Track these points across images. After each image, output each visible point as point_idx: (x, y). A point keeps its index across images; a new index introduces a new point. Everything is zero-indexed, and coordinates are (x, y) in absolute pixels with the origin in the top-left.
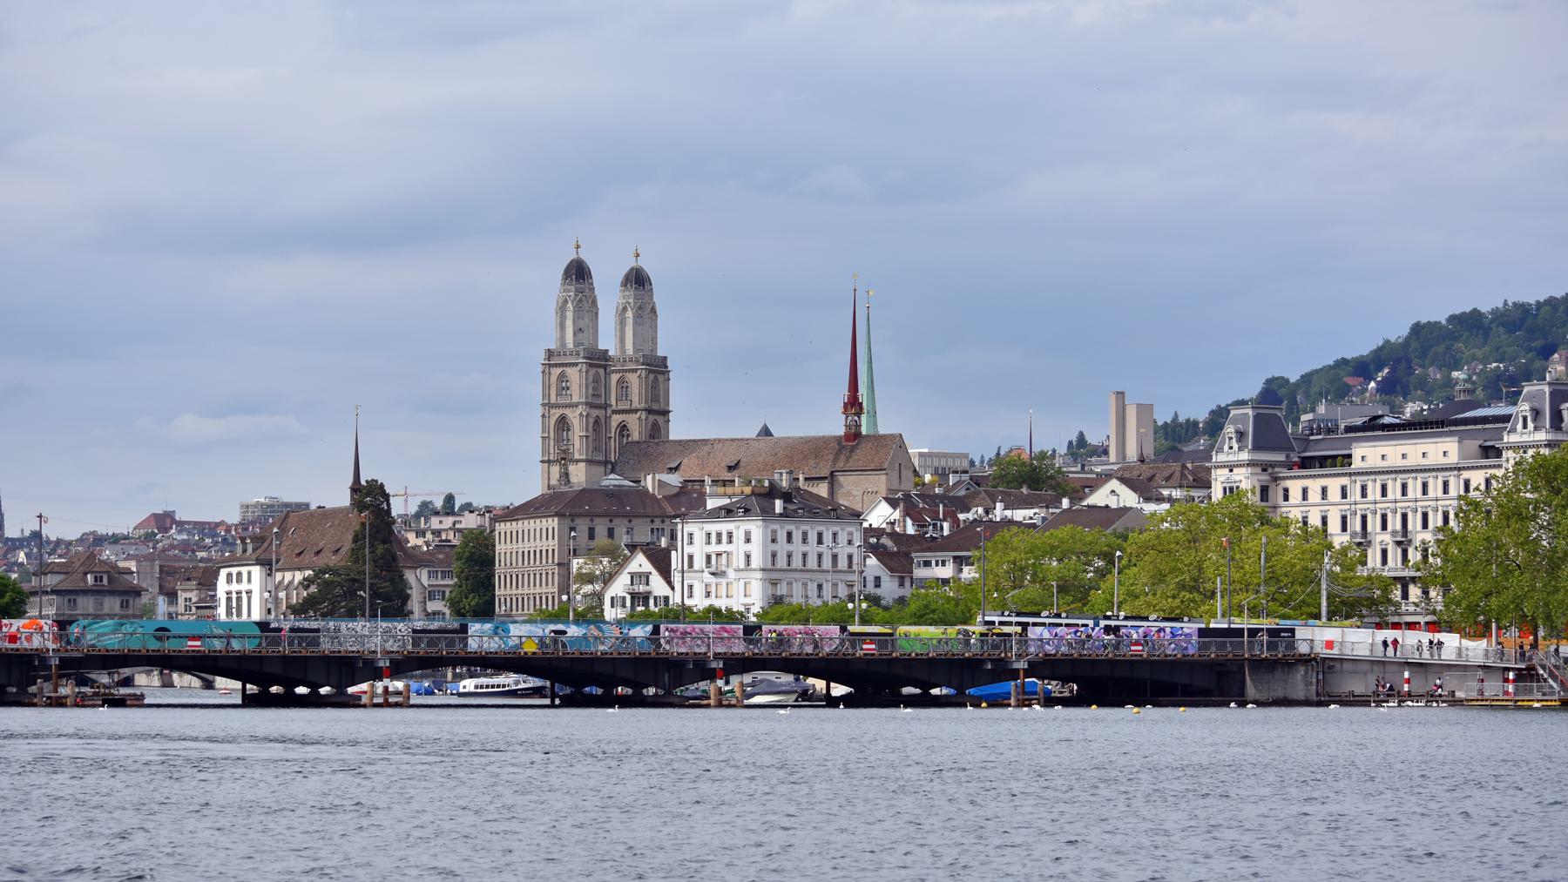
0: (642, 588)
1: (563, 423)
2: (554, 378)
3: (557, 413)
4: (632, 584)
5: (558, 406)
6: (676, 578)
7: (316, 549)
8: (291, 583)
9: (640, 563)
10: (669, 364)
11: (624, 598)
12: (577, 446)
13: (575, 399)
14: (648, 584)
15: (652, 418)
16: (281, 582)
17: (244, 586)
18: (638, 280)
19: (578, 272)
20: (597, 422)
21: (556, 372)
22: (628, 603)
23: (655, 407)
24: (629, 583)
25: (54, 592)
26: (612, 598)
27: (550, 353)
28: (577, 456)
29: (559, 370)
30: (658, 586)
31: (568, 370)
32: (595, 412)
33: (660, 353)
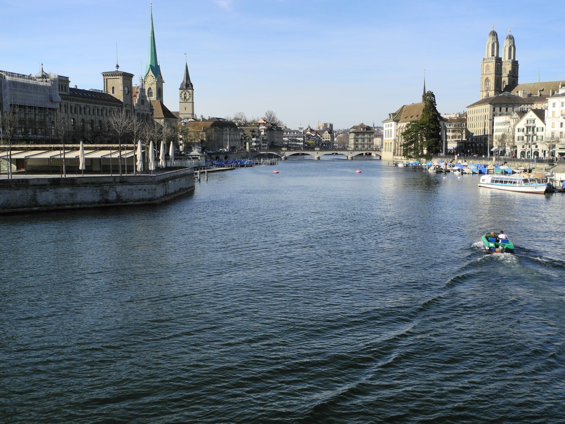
0: (531, 125)
1: (487, 80)
2: (485, 67)
3: (485, 77)
4: (527, 123)
5: (486, 74)
6: (547, 120)
7: (411, 116)
8: (403, 127)
9: (531, 115)
10: (519, 63)
11: (524, 129)
12: (492, 86)
13: (492, 72)
14: (534, 123)
15: (513, 78)
16: (400, 127)
17: (390, 128)
18: (511, 38)
19: (494, 34)
20: (498, 79)
21: (485, 64)
22: (525, 130)
23: (514, 75)
24: (526, 122)
25: (353, 132)
26: (519, 129)
27: (484, 59)
28: (491, 89)
29: (486, 64)
30: (538, 123)
31: (490, 64)
32: (498, 76)
33: (516, 60)
